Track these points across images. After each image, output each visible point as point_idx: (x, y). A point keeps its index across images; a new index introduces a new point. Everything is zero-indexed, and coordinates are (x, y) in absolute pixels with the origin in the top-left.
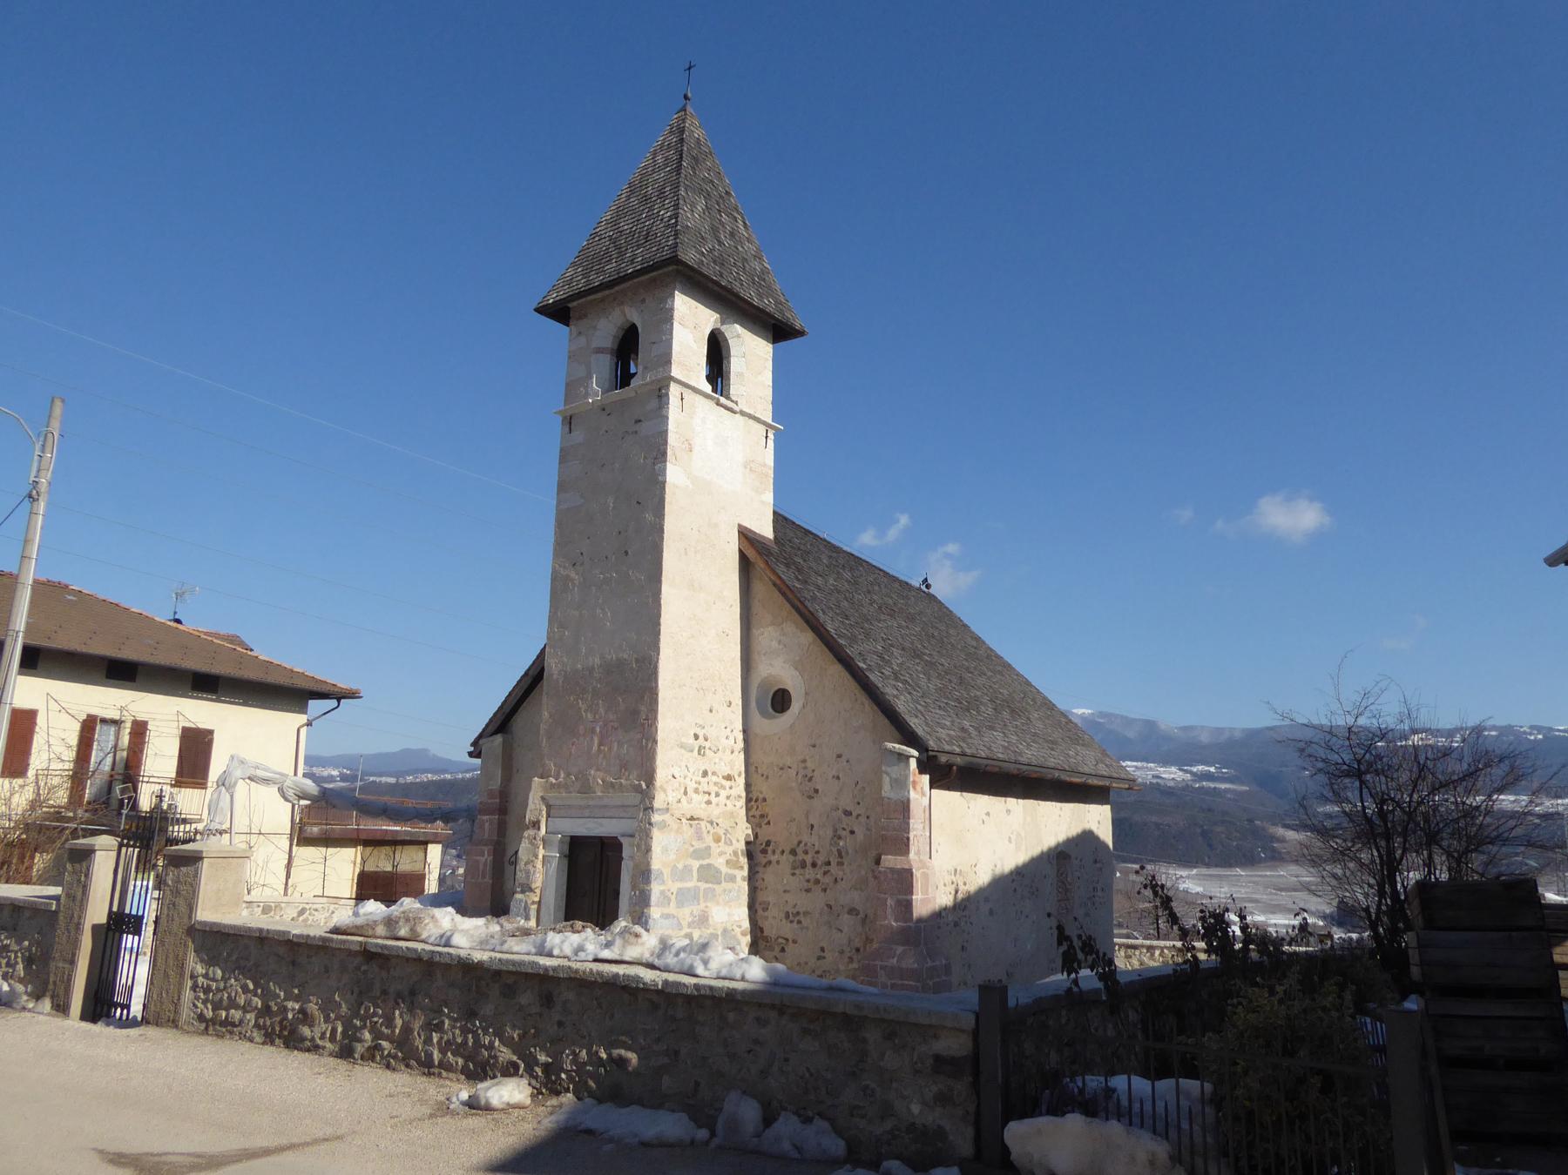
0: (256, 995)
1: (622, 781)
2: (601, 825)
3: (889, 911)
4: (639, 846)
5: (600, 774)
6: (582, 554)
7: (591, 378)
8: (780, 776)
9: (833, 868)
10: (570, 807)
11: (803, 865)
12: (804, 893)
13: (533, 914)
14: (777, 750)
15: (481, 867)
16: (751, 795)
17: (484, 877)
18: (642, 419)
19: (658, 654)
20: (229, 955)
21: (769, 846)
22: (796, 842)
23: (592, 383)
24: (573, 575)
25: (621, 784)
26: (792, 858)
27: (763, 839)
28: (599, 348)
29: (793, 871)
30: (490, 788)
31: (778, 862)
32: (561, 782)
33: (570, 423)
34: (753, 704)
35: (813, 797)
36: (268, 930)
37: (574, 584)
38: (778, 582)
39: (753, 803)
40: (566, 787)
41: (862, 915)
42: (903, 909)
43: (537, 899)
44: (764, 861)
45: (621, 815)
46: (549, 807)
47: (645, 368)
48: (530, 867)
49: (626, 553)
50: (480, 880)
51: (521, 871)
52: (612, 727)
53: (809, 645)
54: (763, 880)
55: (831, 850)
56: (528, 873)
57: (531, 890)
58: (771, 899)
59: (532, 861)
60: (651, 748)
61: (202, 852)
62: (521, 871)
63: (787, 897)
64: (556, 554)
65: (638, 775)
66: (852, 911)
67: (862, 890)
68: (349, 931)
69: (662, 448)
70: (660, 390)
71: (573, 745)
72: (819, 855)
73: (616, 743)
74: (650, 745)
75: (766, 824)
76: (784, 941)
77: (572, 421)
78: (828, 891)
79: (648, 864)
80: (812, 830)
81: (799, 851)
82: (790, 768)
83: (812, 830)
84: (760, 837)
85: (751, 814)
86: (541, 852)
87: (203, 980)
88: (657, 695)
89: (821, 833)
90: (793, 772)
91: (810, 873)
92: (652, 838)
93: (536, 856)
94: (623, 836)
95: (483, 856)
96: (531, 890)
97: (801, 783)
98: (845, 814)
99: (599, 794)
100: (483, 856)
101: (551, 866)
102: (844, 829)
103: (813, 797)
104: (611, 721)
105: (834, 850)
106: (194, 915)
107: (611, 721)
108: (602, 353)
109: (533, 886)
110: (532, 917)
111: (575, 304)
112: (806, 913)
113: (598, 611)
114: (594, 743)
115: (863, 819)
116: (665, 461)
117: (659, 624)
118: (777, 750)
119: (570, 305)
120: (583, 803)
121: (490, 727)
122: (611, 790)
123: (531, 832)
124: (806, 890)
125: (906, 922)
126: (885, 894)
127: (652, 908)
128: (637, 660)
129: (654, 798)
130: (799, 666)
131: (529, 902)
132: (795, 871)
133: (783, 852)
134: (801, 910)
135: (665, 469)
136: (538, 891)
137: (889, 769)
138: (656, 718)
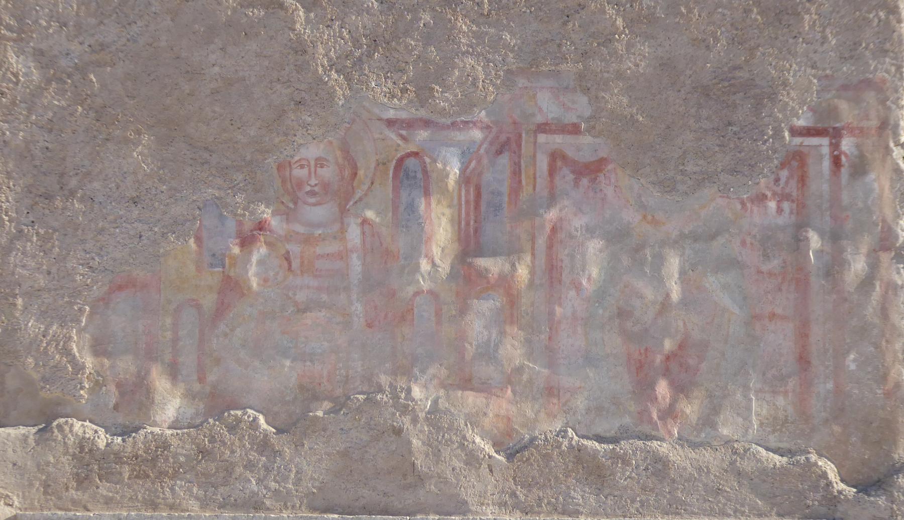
1: (663, 448)
52: (556, 157)
60: (867, 283)
65: (776, 424)
71: (246, 242)
73: (594, 246)
74: (858, 265)
104: (543, 128)
107: (543, 128)
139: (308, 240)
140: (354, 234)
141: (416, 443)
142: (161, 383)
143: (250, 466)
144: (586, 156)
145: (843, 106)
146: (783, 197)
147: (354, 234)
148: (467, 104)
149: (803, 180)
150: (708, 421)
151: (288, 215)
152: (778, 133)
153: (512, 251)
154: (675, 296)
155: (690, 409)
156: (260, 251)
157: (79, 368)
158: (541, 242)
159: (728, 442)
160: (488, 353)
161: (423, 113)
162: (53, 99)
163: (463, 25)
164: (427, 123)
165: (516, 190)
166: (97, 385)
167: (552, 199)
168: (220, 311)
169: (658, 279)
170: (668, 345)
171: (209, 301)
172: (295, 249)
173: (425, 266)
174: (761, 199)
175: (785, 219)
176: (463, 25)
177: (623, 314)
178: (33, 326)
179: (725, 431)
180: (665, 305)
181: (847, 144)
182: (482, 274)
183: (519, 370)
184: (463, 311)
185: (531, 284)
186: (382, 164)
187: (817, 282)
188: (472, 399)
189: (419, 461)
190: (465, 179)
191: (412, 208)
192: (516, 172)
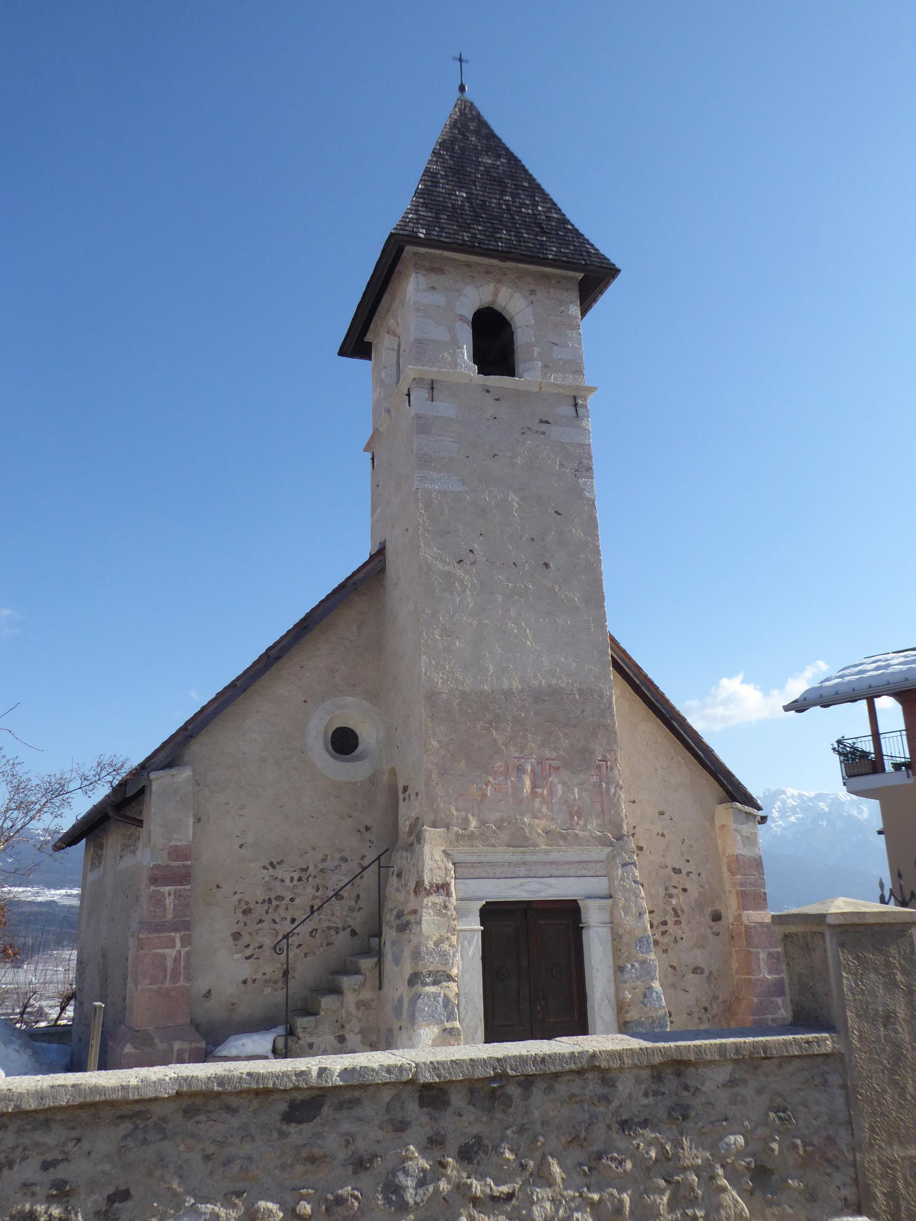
1: (577, 831)
2: (550, 886)
3: (762, 963)
5: (543, 823)
9: (671, 928)
10: (491, 864)
15: (169, 964)
17: (175, 976)
18: (550, 420)
24: (460, 573)
25: (577, 835)
30: (172, 844)
33: (433, 388)
41: (707, 972)
42: (775, 961)
45: (579, 873)
47: (545, 366)
48: (445, 946)
49: (546, 565)
50: (167, 984)
52: (550, 765)
55: (665, 909)
56: (444, 955)
57: (450, 978)
60: (615, 794)
65: (598, 825)
66: (696, 970)
67: (704, 947)
69: (585, 462)
70: (575, 398)
71: (487, 785)
73: (560, 786)
74: (613, 790)
78: (670, 951)
95: (173, 947)
96: (450, 978)
98: (675, 873)
99: (543, 847)
100: (173, 947)
101: (470, 943)
102: (675, 887)
104: (547, 759)
105: (669, 909)
107: (547, 759)
113: (510, 624)
115: (694, 876)
120: (514, 859)
121: (160, 756)
122: (562, 842)
125: (778, 974)
126: (757, 948)
128: (581, 692)
137: (739, 827)
139: (499, 785)
140: (509, 784)
141: (527, 831)
142: (471, 818)
143: (492, 837)
146: (597, 775)
147: (509, 784)
149: (601, 772)
150: (585, 825)
151: (495, 779)
152: (595, 761)
153: (542, 787)
154: (577, 798)
155: (581, 823)
156: (490, 787)
157: (453, 815)
158: (549, 785)
159: (589, 830)
160: (540, 810)
161: (522, 756)
164: (523, 758)
165: (542, 774)
166: (457, 818)
167: (550, 775)
168: (482, 801)
169: (573, 793)
170: (576, 808)
171: (479, 799)
172: (496, 786)
173: (525, 791)
174: (593, 775)
177: (566, 801)
178: (442, 805)
179: (589, 828)
180: (575, 799)
182: (537, 793)
183: (546, 814)
184: (534, 801)
185: (547, 795)
186: (514, 767)
187: (605, 794)
188: (537, 821)
190: (532, 771)
191: (521, 777)
192: (542, 769)
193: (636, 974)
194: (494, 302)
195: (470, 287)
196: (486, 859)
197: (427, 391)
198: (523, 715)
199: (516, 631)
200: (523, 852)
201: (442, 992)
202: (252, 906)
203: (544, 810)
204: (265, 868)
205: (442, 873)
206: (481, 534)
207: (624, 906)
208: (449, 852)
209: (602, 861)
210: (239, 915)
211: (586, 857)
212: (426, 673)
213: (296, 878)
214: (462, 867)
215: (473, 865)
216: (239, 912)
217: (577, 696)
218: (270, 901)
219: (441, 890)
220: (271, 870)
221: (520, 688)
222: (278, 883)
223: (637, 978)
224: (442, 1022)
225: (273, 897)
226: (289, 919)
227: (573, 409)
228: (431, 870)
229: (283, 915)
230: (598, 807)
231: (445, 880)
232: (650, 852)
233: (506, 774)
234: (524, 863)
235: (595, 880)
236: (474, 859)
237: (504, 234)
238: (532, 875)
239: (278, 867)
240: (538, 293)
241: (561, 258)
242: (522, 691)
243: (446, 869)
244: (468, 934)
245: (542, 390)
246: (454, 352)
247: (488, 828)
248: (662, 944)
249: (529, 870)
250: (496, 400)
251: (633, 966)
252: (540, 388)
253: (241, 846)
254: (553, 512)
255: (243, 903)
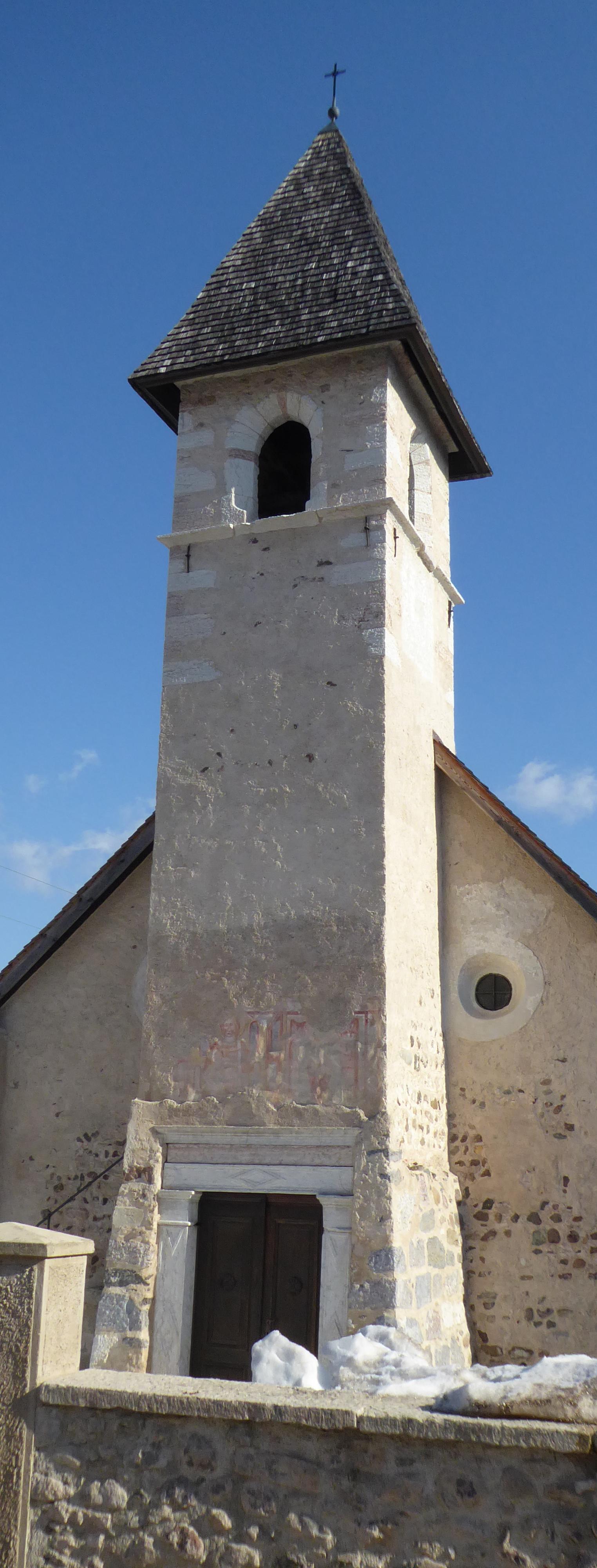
0: (241, 1537)
1: (317, 1107)
2: (277, 1176)
4: (363, 1211)
5: (275, 1095)
6: (219, 754)
7: (227, 493)
8: (505, 1103)
11: (554, 1238)
12: (559, 1281)
13: (144, 1319)
14: (498, 1065)
16: (454, 1131)
18: (332, 560)
19: (383, 913)
20: (149, 1459)
21: (490, 1208)
22: (538, 1204)
23: (230, 500)
24: (203, 784)
25: (316, 1112)
26: (532, 1227)
27: (478, 1196)
28: (239, 450)
29: (535, 1247)
31: (508, 1233)
32: (190, 1106)
33: (188, 556)
34: (455, 996)
35: (565, 1137)
36: (276, 1407)
37: (205, 801)
38: (505, 818)
39: (458, 1143)
40: (201, 1114)
43: (150, 1295)
44: (483, 1231)
45: (317, 1161)
46: (166, 1146)
47: (334, 486)
48: (137, 1243)
49: (310, 757)
51: (118, 1249)
52: (292, 1021)
53: (549, 911)
54: (483, 1259)
56: (133, 1253)
57: (140, 1280)
58: (498, 1288)
59: (141, 1233)
60: (373, 1057)
61: (43, 1247)
62: (118, 1249)
63: (526, 1285)
64: (166, 751)
65: (349, 1099)
68: (515, 1411)
70: (367, 519)
71: (212, 1048)
72: (581, 1223)
73: (301, 1048)
74: (371, 1052)
75: (483, 1175)
76: (525, 1354)
77: (191, 553)
79: (387, 1240)
80: (565, 1185)
81: (545, 1215)
82: (521, 1091)
83: (565, 1185)
84: (471, 1196)
85: (456, 1158)
86: (156, 1218)
87: (71, 1509)
88: (383, 975)
89: (583, 1190)
90: (527, 1098)
91: (565, 1250)
92: (390, 1198)
93: (148, 1225)
94: (325, 1194)
96: (140, 1280)
97: (542, 1116)
99: (271, 1126)
101: (174, 1241)
103: (565, 1137)
104: (289, 1013)
106: (28, 1375)
107: (289, 1013)
108: (243, 457)
109: (144, 1274)
110: (143, 1325)
111: (190, 381)
112: (563, 1312)
113: (258, 842)
114: (256, 1046)
116: (382, 625)
117: (382, 867)
118: (498, 1065)
119: (179, 384)
120: (236, 1140)
122: (296, 1121)
123: (136, 1186)
124: (561, 1277)
127: (396, 1310)
128: (340, 921)
129: (387, 1136)
130: (531, 942)
131: (138, 1300)
132: (541, 1247)
133: (516, 1218)
134: (555, 1307)
135: (381, 637)
136: (151, 1281)
138: (381, 1011)
139: (227, 1047)
140: (239, 1046)
141: (253, 1106)
142: (190, 1090)
143: (212, 1112)
144: (300, 1021)
145: (369, 1004)
146: (352, 1032)
147: (239, 1046)
148: (269, 1007)
149: (358, 1027)
150: (330, 1099)
151: (222, 1040)
152: (351, 1013)
153: (280, 1050)
154: (322, 1062)
155: (325, 1095)
156: (215, 1051)
157: (170, 1085)
158: (288, 1047)
159: (335, 1105)
160: (273, 1080)
161: (257, 1010)
162: (164, 1009)
163: (268, 983)
164: (258, 1012)
166: (175, 1089)
168: (205, 1068)
169: (318, 1057)
170: (320, 1077)
172: (224, 1050)
173: (257, 1054)
174: (346, 1033)
175: (352, 1038)
176: (268, 983)
177: (309, 1068)
178: (159, 1073)
179: (334, 1102)
180: (320, 1065)
181: (370, 1016)
182: (272, 1057)
183: (281, 1085)
184: (267, 1067)
185: (285, 1060)
187: (360, 1057)
188: (268, 1093)
189: (254, 1111)
190: (268, 1028)
191: (254, 1037)
193: (364, 1297)
194: (285, 414)
195: (245, 408)
196: (203, 1140)
197: (183, 561)
198: (263, 958)
199: (263, 850)
200: (247, 1133)
201: (127, 1295)
202: (64, 1181)
203: (279, 1079)
204: (79, 1140)
205: (145, 1155)
206: (232, 731)
207: (362, 1206)
208: (160, 1130)
209: (348, 1147)
210: (51, 1192)
211: (326, 1140)
212: (154, 914)
213: (111, 1152)
214: (175, 1148)
215: (189, 1146)
216: (51, 1188)
217: (335, 928)
218: (82, 1177)
219: (143, 1176)
220: (86, 1143)
221: (262, 923)
222: (92, 1157)
223: (365, 1304)
224: (124, 1330)
225: (85, 1173)
226: (101, 1199)
227: (363, 535)
228: (133, 1151)
229: (95, 1193)
230: (350, 1074)
231: (148, 1163)
232: (586, 1133)
233: (237, 1034)
234: (249, 1146)
235: (336, 1170)
236: (190, 1139)
237: (276, 328)
238: (257, 1162)
239: (93, 1139)
240: (332, 387)
241: (335, 336)
242: (266, 926)
243: (151, 1150)
244: (171, 1229)
245: (324, 519)
246: (219, 501)
247: (208, 1101)
248: (591, 1266)
249: (254, 1155)
250: (265, 549)
251: (362, 1286)
252: (320, 519)
253: (57, 1115)
254: (325, 684)
255: (55, 1177)
